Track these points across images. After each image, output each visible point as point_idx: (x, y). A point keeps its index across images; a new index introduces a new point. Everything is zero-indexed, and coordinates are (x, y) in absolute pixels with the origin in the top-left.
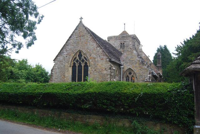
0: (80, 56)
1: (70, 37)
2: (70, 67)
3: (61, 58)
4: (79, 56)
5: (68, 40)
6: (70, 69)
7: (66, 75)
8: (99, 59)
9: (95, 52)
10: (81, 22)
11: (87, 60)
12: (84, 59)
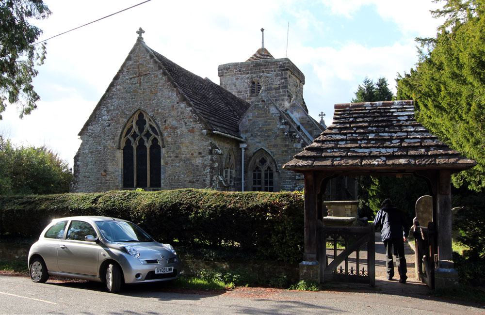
0: (141, 122)
1: (116, 78)
2: (119, 148)
3: (96, 128)
4: (137, 123)
5: (112, 85)
6: (119, 155)
7: (110, 168)
8: (184, 129)
9: (174, 113)
10: (140, 40)
11: (156, 133)
12: (151, 132)
